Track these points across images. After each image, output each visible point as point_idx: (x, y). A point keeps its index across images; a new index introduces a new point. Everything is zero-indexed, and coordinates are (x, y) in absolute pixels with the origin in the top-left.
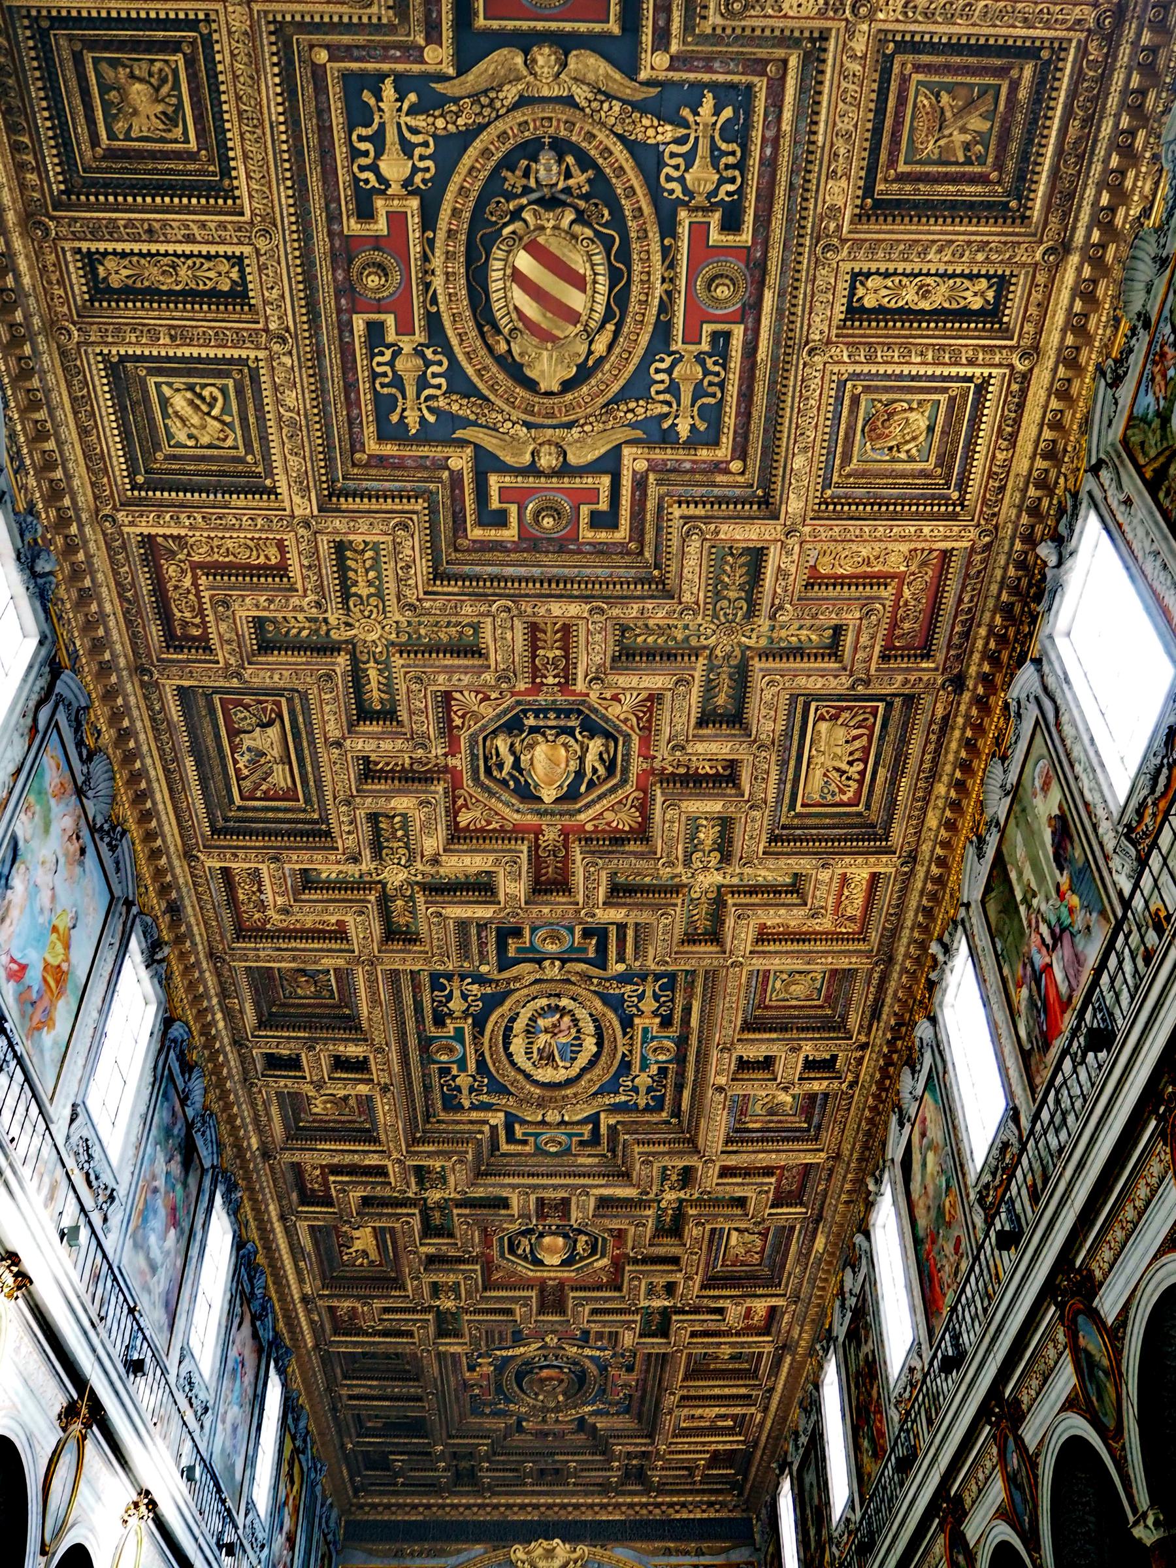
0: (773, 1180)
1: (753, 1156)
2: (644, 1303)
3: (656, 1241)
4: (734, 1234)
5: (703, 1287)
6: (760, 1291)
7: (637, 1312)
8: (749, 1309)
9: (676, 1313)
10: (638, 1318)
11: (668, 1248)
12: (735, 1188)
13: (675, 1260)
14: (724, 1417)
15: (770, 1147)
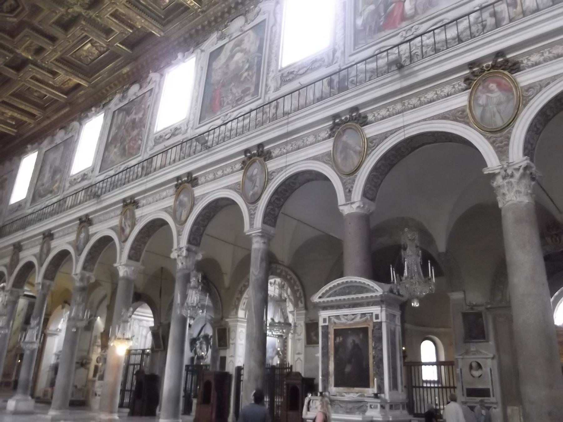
0: (131, 31)
1: (135, 15)
2: (18, 51)
3: (53, 26)
4: (89, 45)
5: (56, 60)
6: (80, 75)
7: (11, 51)
8: (70, 80)
9: (32, 64)
10: (12, 56)
11: (57, 32)
12: (113, 24)
13: (53, 39)
14: (12, 118)
15: (144, 15)
